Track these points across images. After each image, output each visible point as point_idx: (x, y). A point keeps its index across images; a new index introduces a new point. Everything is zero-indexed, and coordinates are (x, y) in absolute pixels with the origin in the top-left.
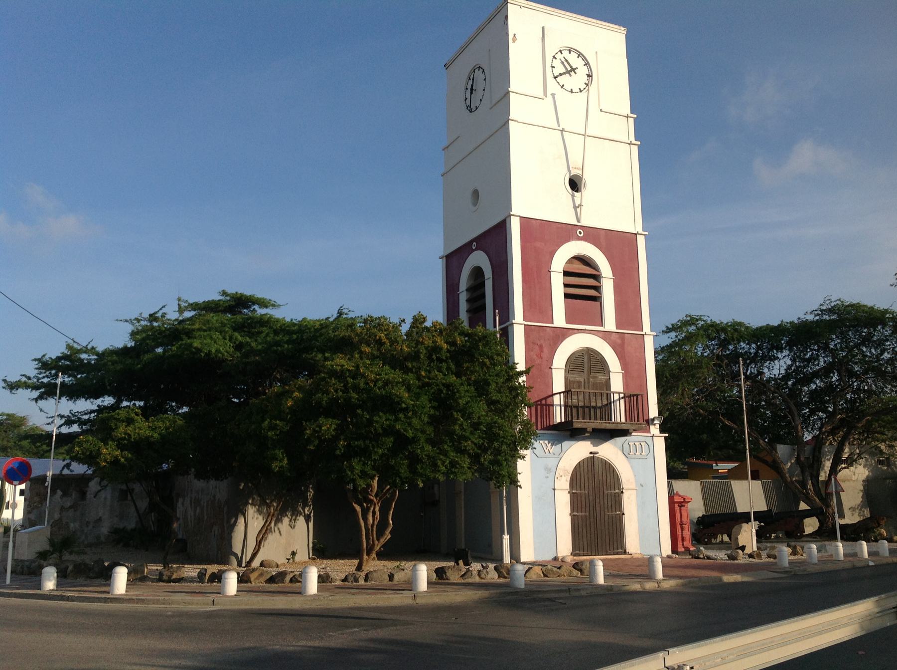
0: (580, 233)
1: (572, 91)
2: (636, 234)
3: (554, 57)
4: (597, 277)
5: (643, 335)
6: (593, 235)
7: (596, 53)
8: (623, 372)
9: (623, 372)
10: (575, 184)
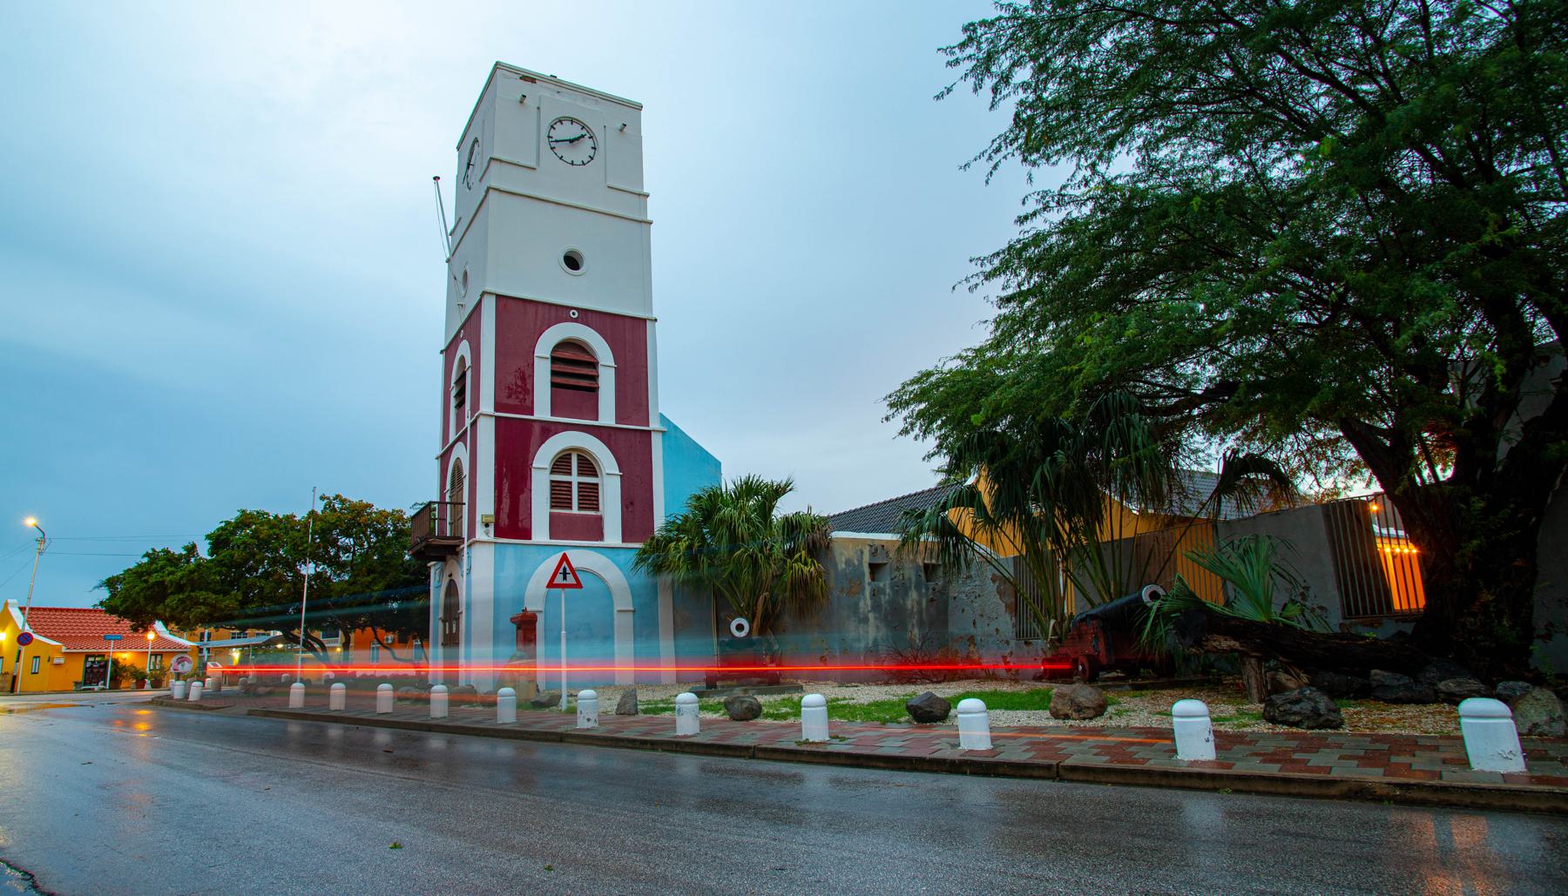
1: (572, 164)
2: (645, 320)
3: (552, 127)
4: (594, 365)
5: (649, 432)
6: (587, 317)
10: (572, 262)
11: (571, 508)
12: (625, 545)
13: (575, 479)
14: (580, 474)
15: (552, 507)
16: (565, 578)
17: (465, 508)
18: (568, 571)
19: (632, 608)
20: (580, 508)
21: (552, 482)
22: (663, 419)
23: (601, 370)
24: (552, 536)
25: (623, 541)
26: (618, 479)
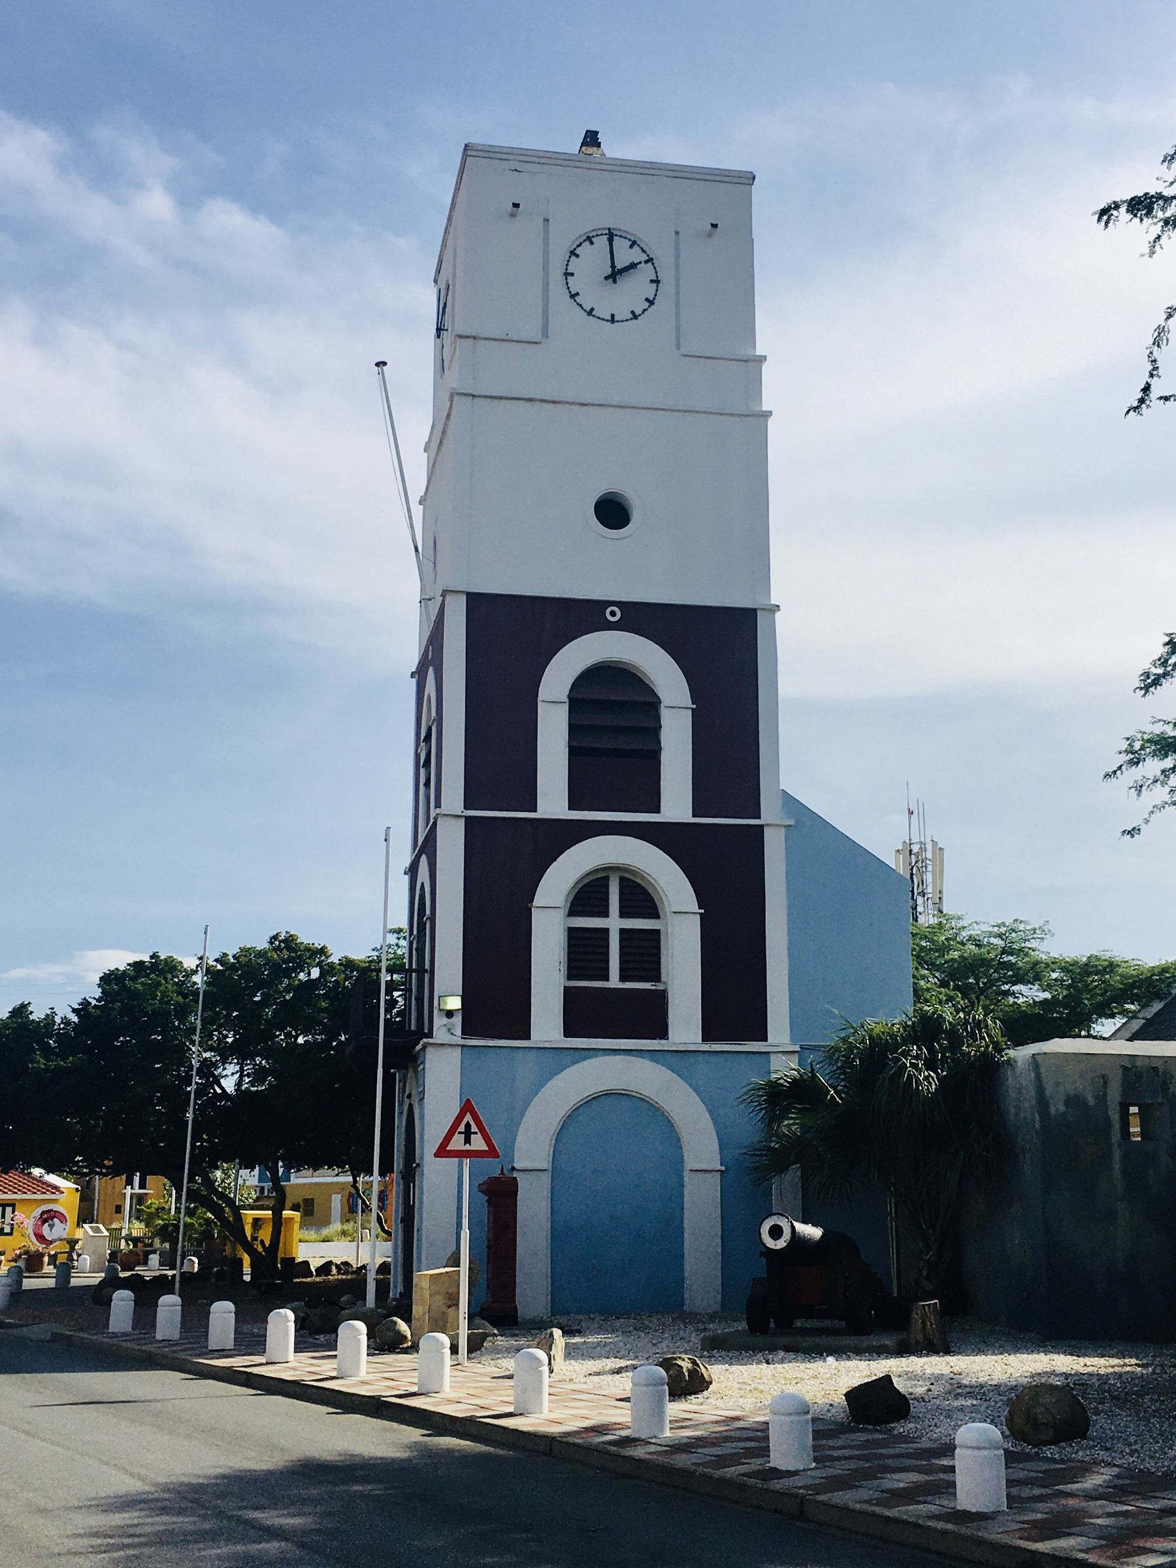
0: (614, 615)
4: (650, 705)
5: (761, 827)
7: (677, 233)
8: (702, 911)
9: (702, 911)
12: (706, 1047)
13: (614, 923)
14: (623, 915)
15: (570, 977)
16: (467, 1141)
17: (427, 976)
18: (474, 1128)
19: (719, 1167)
20: (623, 979)
21: (571, 931)
22: (790, 803)
23: (666, 716)
24: (570, 1030)
25: (706, 1038)
26: (697, 920)
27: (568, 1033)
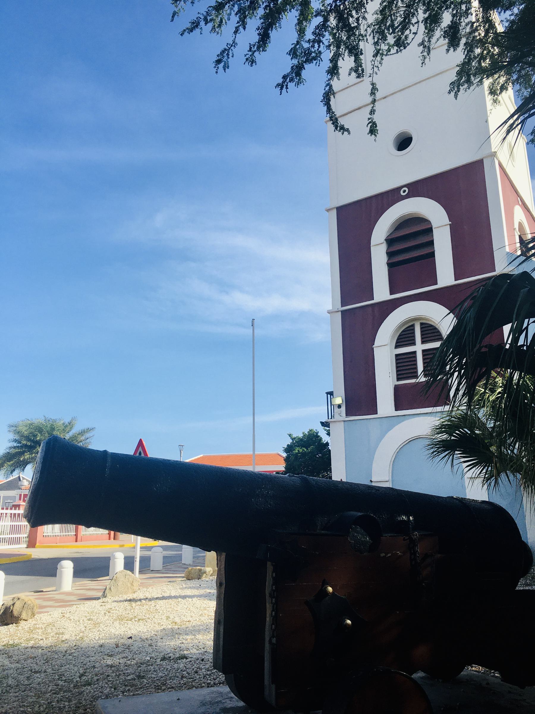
4: (429, 231)
11: (416, 377)
14: (423, 342)
15: (398, 379)
21: (397, 355)
27: (397, 409)
